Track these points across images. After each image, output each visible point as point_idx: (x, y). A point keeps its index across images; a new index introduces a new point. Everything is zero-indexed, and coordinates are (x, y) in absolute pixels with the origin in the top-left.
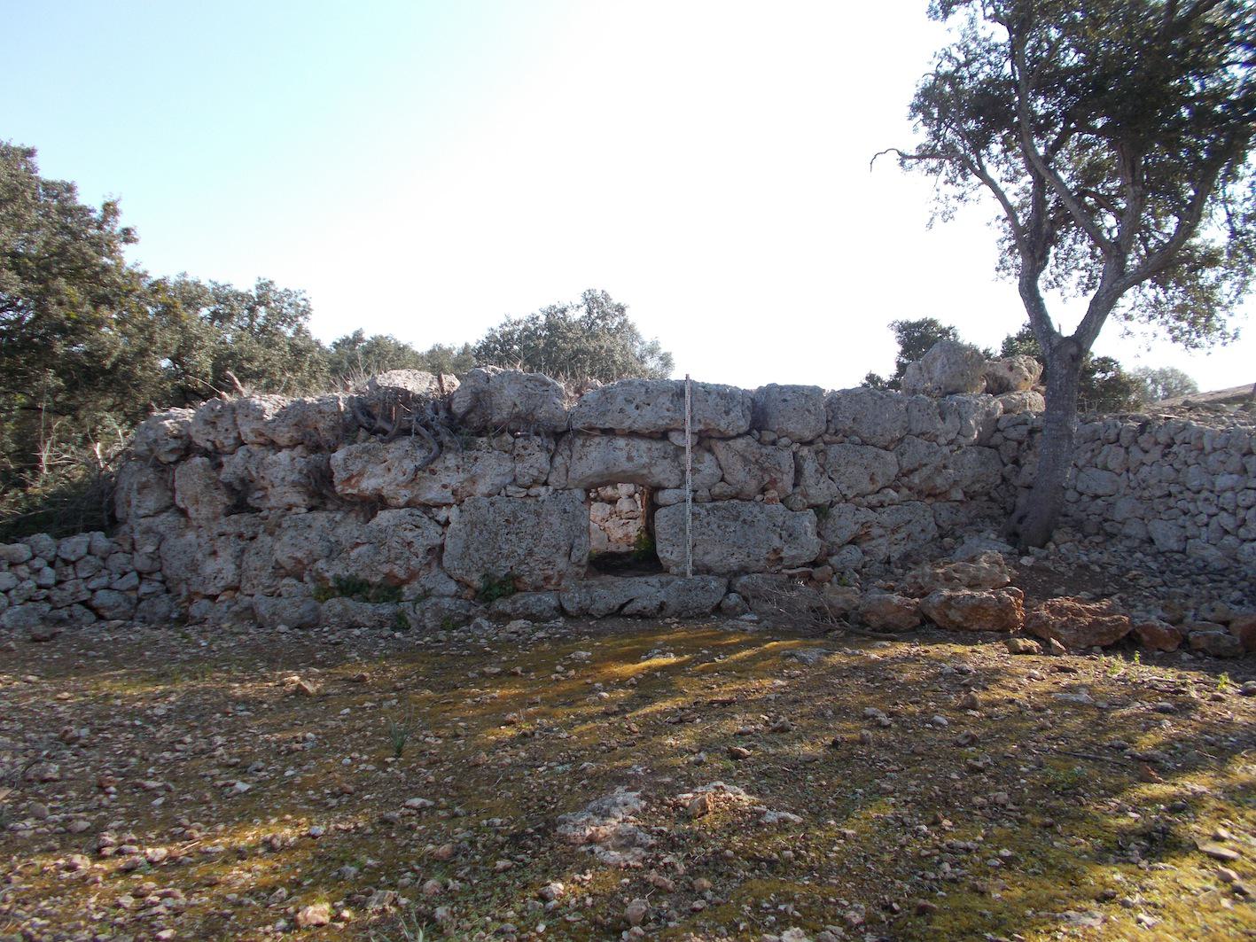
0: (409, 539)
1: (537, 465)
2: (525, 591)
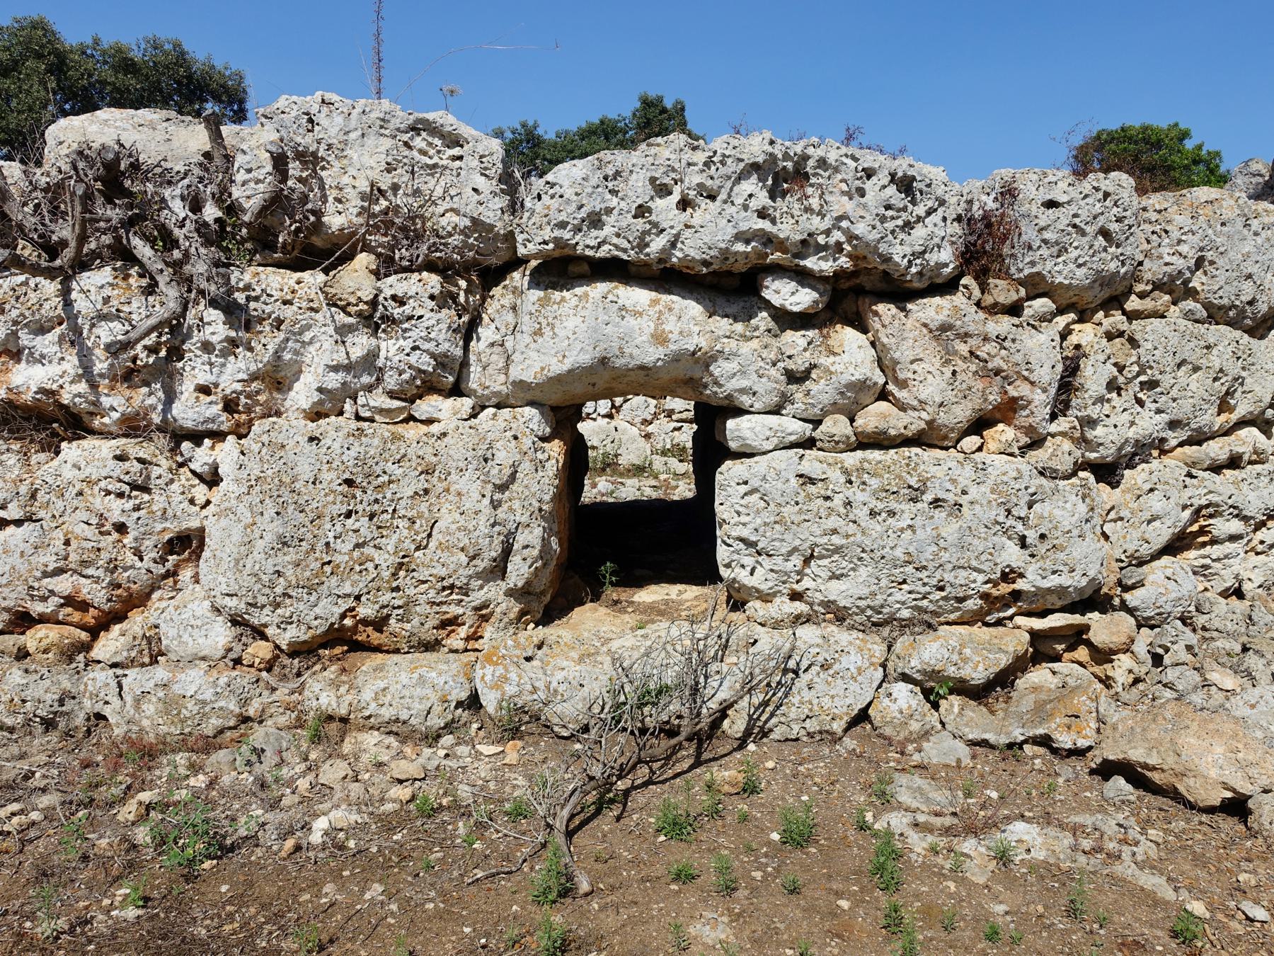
0: (116, 517)
1: (430, 346)
2: (397, 651)
